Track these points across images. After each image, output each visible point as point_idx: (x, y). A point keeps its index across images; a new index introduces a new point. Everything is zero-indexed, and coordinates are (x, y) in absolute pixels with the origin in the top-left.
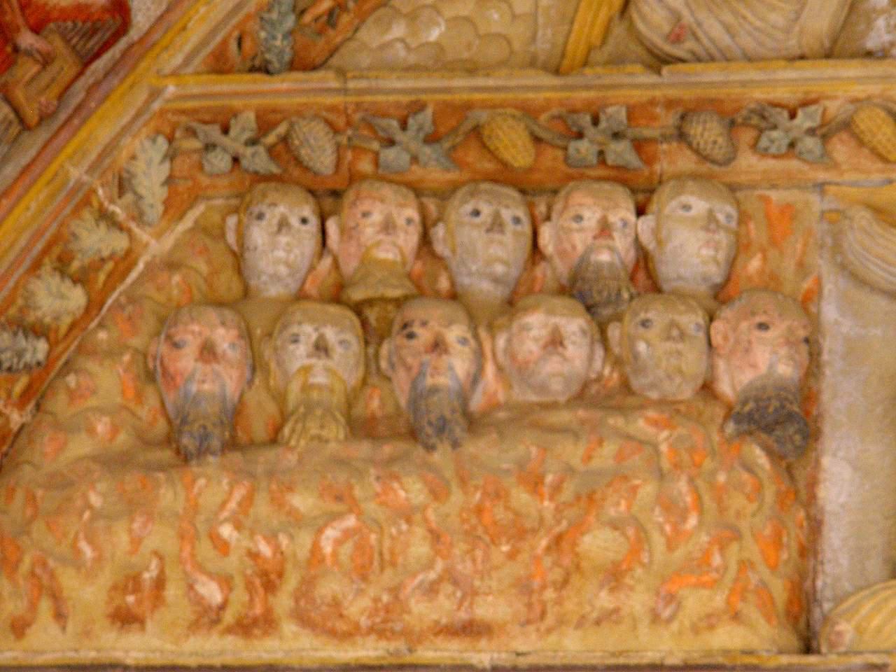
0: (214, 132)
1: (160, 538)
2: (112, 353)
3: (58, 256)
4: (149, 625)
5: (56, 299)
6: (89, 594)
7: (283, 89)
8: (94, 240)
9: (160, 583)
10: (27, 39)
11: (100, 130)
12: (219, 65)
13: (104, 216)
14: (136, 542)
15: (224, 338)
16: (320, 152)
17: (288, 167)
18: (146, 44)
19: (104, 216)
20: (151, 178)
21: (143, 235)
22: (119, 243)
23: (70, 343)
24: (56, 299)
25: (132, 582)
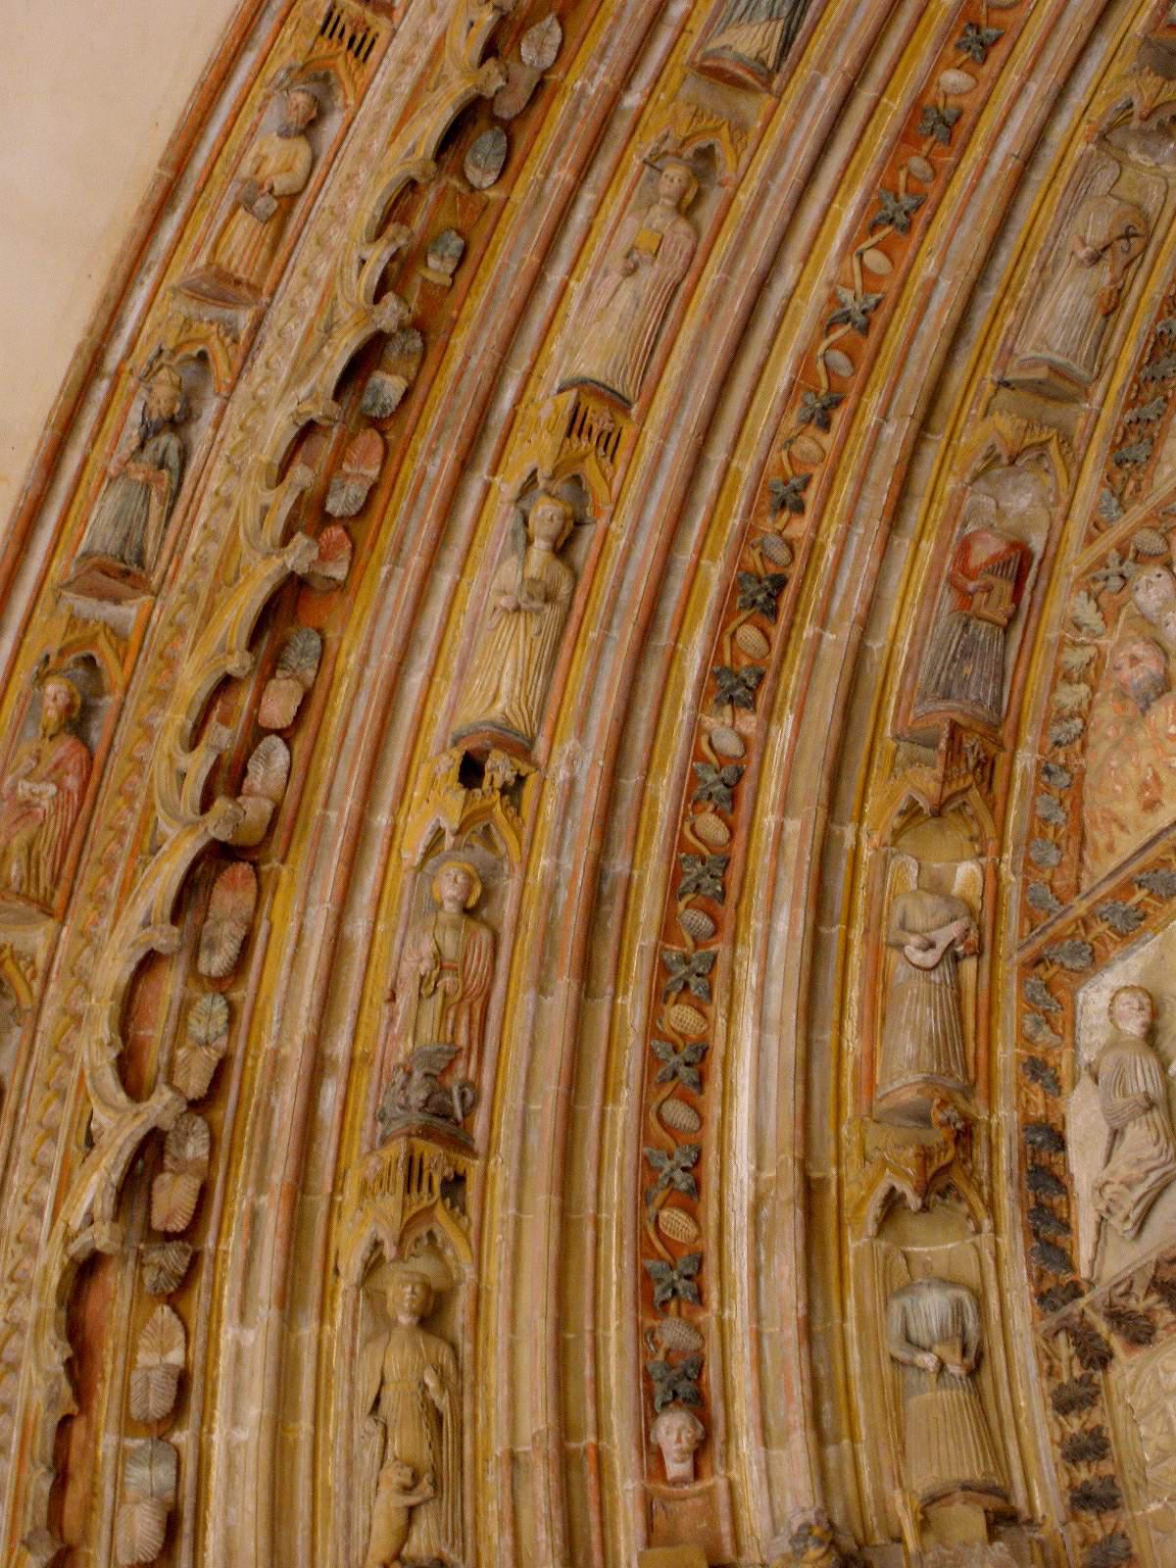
0: (1103, 571)
1: (1146, 756)
2: (1103, 700)
3: (1064, 676)
4: (1165, 801)
5: (1071, 696)
6: (1129, 808)
7: (1120, 529)
8: (1075, 658)
9: (1156, 777)
10: (971, 586)
11: (1054, 610)
12: (1090, 540)
13: (1074, 644)
14: (1138, 767)
15: (1139, 650)
16: (1150, 541)
17: (1141, 558)
18: (1051, 557)
19: (1074, 644)
20: (1088, 613)
21: (1101, 642)
22: (1091, 651)
23: (1085, 713)
24: (1071, 696)
25: (1145, 786)
